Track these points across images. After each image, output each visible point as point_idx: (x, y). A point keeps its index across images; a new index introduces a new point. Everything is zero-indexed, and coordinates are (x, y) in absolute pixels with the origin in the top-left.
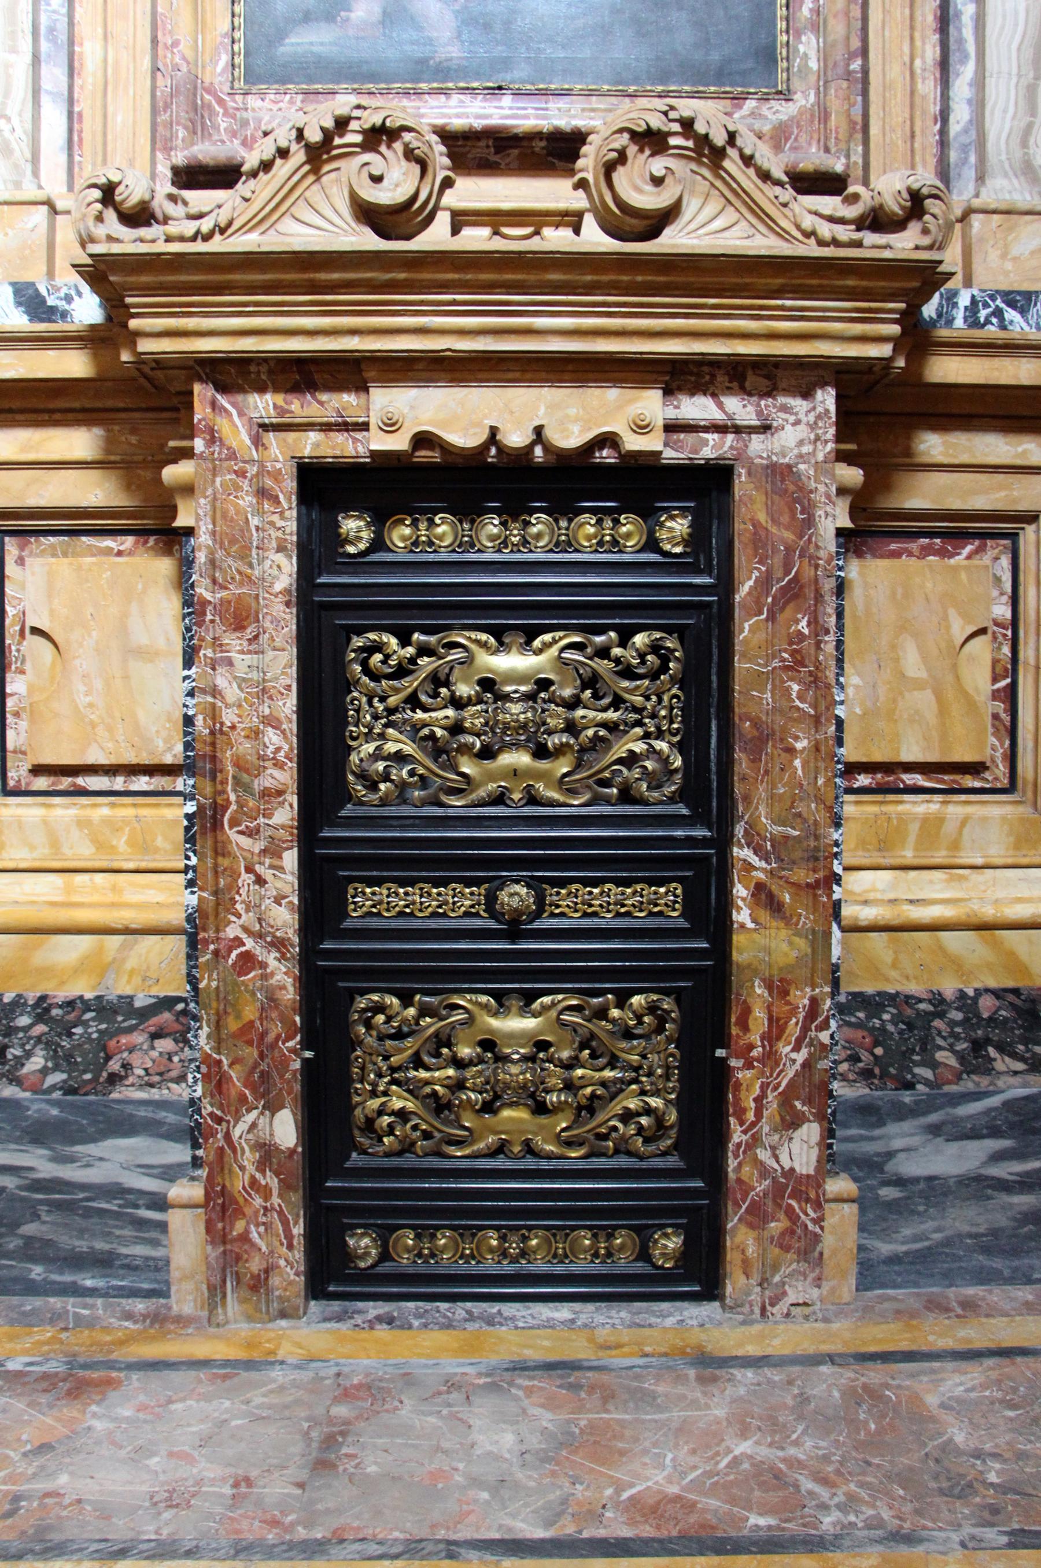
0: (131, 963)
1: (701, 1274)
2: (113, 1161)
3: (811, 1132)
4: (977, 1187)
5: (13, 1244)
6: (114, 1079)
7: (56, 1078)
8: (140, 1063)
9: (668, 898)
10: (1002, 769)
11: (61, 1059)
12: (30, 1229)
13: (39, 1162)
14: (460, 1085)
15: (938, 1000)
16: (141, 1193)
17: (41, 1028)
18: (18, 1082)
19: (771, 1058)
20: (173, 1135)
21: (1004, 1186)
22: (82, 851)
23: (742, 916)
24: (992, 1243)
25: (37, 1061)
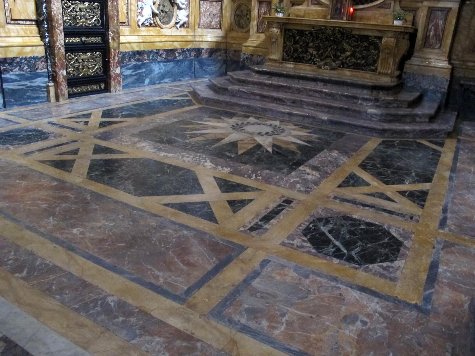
0: (37, 51)
1: (107, 89)
2: (40, 82)
3: (119, 68)
4: (131, 76)
5: (25, 97)
6: (37, 69)
7: (29, 70)
8: (40, 66)
9: (98, 39)
10: (127, 23)
11: (29, 67)
12: (28, 94)
13: (28, 83)
14: (79, 66)
15: (126, 52)
16: (42, 86)
17: (26, 62)
18: (23, 71)
19: (114, 59)
20: (45, 77)
21: (133, 75)
22: (22, 34)
23: (111, 41)
24: (133, 83)
25: (26, 67)
